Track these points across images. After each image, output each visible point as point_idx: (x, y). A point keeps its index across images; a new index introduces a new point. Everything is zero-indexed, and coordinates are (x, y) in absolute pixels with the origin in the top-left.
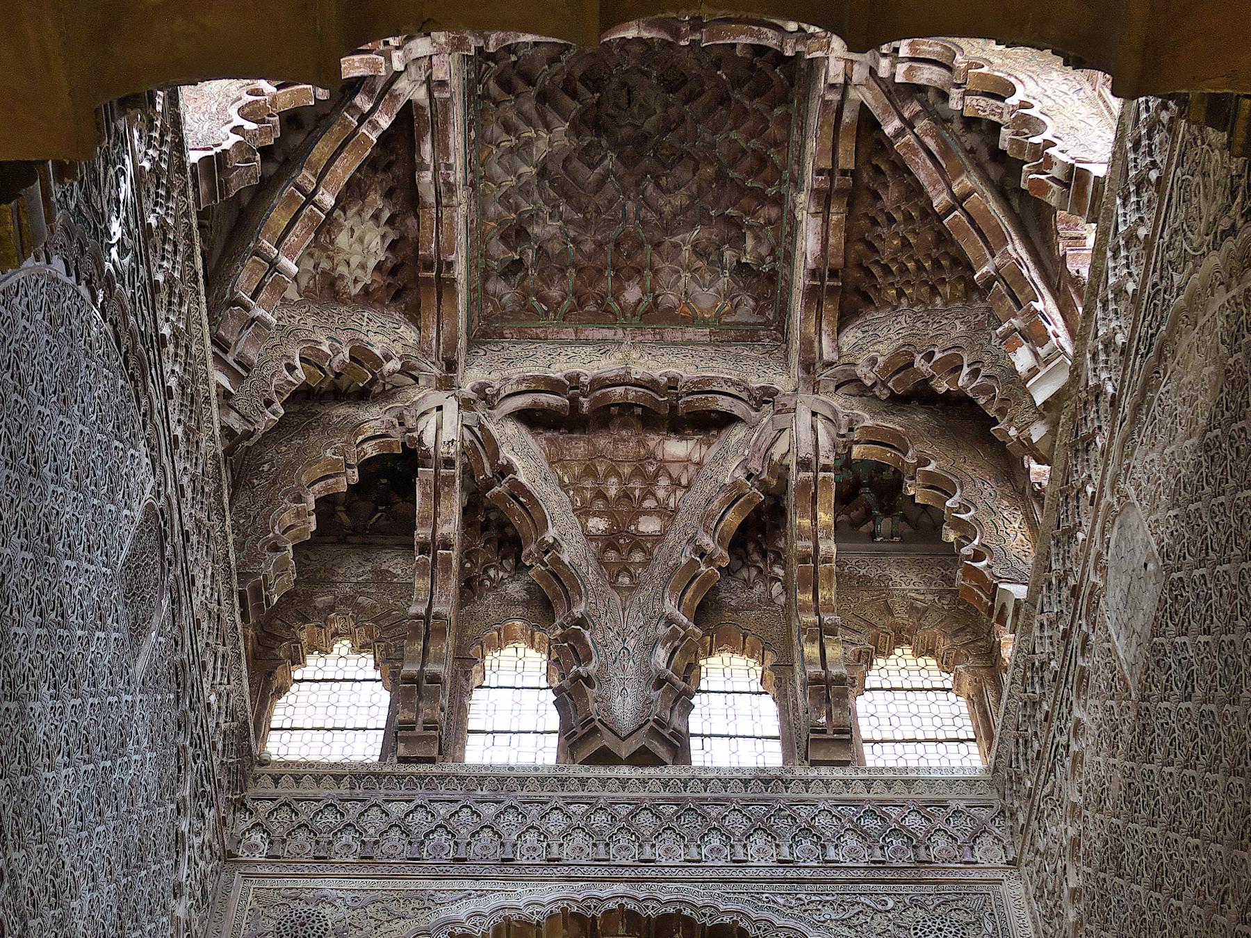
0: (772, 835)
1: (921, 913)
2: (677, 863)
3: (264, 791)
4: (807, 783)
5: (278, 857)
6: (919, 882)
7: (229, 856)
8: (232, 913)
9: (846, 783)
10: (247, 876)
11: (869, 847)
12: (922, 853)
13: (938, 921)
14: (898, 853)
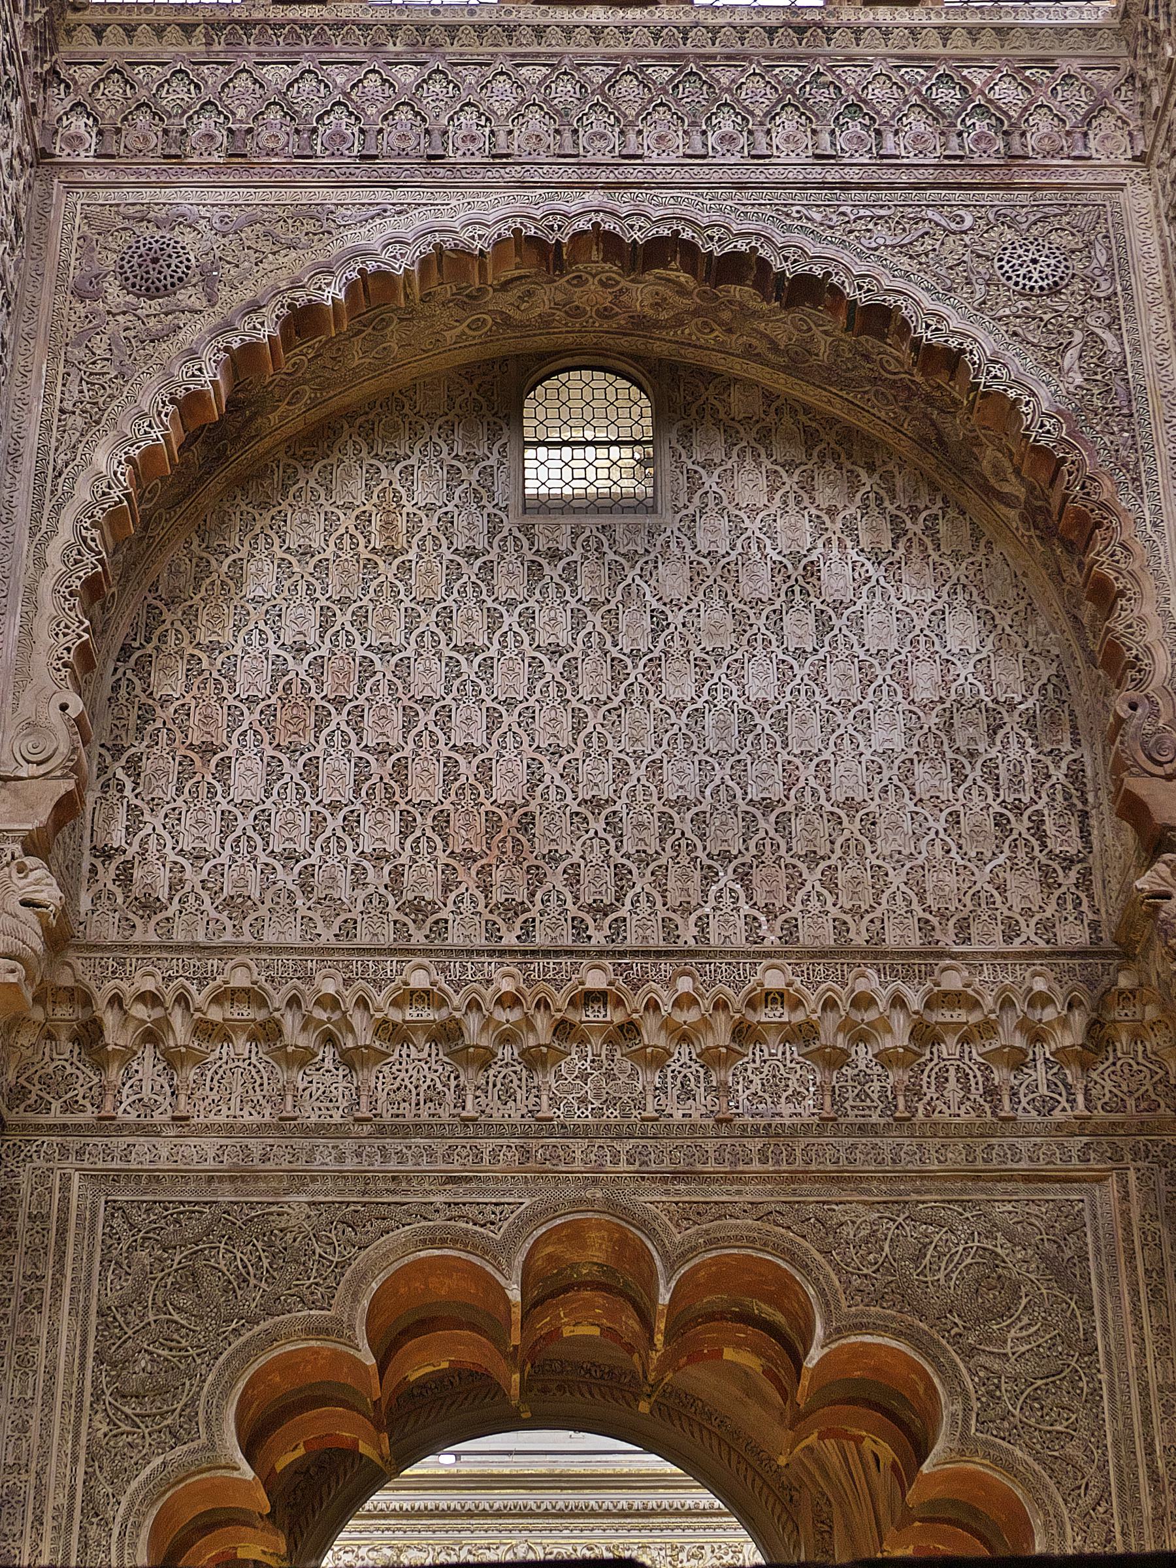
0: (802, 107)
1: (1009, 235)
3: (82, 49)
4: (858, 32)
5: (112, 157)
6: (1009, 187)
7: (43, 156)
8: (55, 244)
9: (913, 31)
10: (70, 186)
11: (942, 133)
12: (1016, 140)
13: (1032, 248)
14: (976, 138)
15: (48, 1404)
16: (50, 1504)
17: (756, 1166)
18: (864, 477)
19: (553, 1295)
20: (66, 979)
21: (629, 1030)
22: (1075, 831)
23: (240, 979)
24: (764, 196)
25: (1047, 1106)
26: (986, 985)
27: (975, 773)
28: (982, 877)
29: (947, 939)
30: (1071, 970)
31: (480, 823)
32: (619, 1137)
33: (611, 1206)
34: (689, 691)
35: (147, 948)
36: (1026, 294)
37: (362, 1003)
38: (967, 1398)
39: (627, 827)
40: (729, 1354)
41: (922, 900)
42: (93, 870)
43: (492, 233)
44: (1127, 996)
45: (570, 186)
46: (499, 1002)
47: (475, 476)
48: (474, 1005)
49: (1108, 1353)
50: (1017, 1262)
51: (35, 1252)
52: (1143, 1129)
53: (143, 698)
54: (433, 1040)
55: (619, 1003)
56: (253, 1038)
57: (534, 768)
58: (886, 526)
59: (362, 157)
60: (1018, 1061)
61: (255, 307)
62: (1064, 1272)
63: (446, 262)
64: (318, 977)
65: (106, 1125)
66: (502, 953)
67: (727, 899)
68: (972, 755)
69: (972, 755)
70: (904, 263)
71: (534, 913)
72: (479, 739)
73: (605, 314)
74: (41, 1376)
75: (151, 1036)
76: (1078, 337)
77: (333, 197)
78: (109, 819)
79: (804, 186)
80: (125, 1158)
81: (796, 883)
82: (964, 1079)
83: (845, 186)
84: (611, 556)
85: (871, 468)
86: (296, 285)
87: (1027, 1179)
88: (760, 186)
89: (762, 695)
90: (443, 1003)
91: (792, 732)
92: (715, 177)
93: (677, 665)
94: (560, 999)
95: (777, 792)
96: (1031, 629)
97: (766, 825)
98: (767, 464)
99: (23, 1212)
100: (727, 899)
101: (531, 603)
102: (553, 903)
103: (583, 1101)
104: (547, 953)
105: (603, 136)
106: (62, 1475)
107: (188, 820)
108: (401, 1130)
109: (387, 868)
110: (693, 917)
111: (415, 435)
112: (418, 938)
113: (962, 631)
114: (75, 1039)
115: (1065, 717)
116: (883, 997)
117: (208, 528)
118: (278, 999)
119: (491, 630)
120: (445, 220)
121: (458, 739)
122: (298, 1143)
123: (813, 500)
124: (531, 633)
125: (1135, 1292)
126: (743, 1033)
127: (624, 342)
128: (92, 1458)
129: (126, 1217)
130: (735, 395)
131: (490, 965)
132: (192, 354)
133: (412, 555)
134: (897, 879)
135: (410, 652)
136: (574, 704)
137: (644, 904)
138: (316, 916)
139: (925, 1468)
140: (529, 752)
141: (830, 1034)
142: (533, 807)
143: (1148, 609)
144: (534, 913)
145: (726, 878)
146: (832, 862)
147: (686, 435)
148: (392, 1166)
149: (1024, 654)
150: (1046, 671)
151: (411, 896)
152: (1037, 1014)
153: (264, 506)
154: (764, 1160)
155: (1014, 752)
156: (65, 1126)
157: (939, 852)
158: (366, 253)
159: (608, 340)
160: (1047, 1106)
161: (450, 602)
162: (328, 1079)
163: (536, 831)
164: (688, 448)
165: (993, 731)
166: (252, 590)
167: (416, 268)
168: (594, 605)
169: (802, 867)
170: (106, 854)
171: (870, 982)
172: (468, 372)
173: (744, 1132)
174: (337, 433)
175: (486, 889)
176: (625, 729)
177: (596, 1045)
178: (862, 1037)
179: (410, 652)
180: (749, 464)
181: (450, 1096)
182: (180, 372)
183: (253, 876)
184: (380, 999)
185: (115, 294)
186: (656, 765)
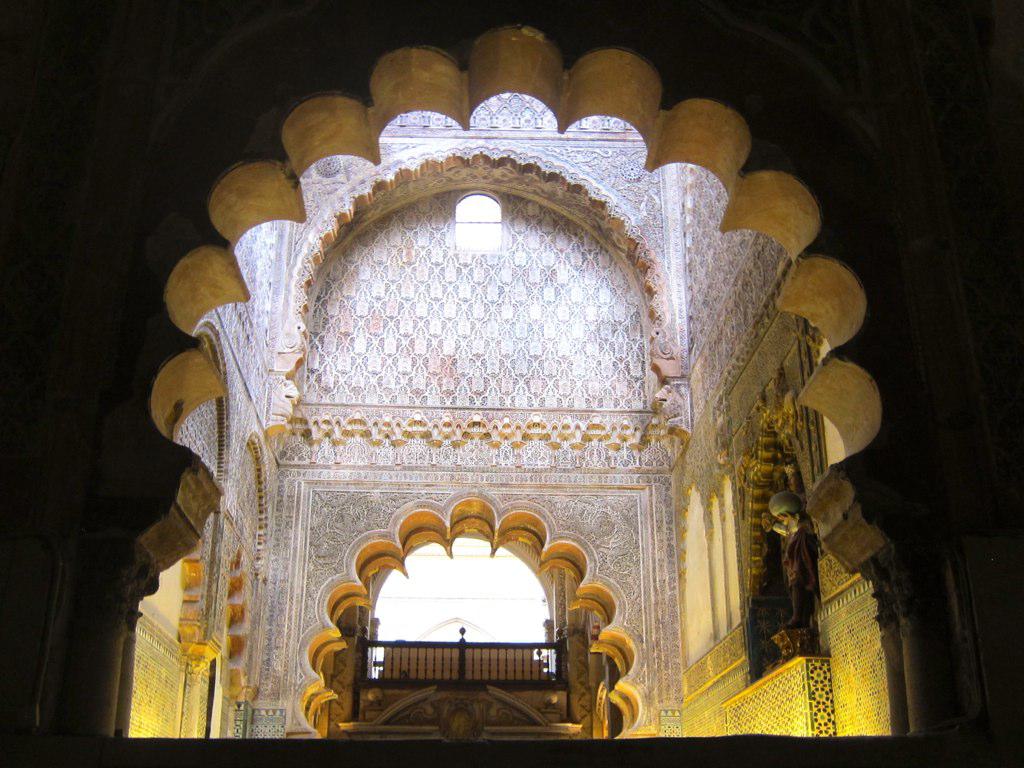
1: (624, 158)
6: (624, 141)
15: (294, 560)
20: (299, 415)
21: (487, 435)
22: (640, 369)
23: (357, 416)
25: (626, 464)
26: (608, 422)
27: (607, 347)
28: (608, 384)
29: (595, 406)
31: (439, 363)
33: (481, 495)
34: (510, 316)
35: (327, 405)
37: (398, 425)
40: (520, 539)
42: (308, 377)
44: (655, 426)
45: (472, 138)
46: (444, 425)
48: (436, 426)
49: (643, 549)
50: (614, 517)
51: (290, 509)
52: (658, 472)
53: (325, 315)
54: (422, 437)
55: (484, 426)
56: (362, 436)
57: (457, 342)
60: (618, 448)
61: (363, 182)
63: (430, 167)
65: (312, 465)
66: (445, 408)
67: (521, 391)
68: (606, 340)
69: (606, 340)
72: (439, 332)
75: (328, 435)
78: (313, 359)
79: (553, 139)
83: (568, 140)
84: (485, 266)
85: (576, 235)
87: (619, 488)
90: (425, 425)
92: (523, 135)
94: (464, 425)
97: (535, 364)
100: (521, 391)
102: (463, 391)
104: (460, 409)
105: (484, 119)
106: (299, 582)
107: (340, 360)
108: (411, 469)
109: (407, 377)
110: (509, 398)
112: (417, 403)
113: (605, 295)
114: (303, 435)
115: (639, 327)
116: (573, 426)
118: (370, 424)
120: (426, 151)
121: (432, 332)
122: (376, 472)
126: (526, 437)
127: (492, 187)
128: (309, 578)
129: (319, 496)
130: (530, 207)
133: (417, 265)
134: (579, 384)
135: (416, 300)
139: (581, 585)
141: (555, 438)
142: (457, 357)
143: (664, 299)
145: (521, 383)
147: (513, 219)
148: (408, 480)
150: (633, 311)
152: (623, 432)
153: (366, 246)
154: (532, 480)
155: (621, 339)
157: (593, 374)
159: (485, 186)
160: (626, 464)
162: (387, 450)
163: (458, 365)
167: (419, 168)
168: (479, 284)
170: (312, 371)
171: (568, 421)
172: (437, 196)
174: (391, 220)
175: (440, 385)
176: (489, 329)
177: (477, 440)
178: (565, 439)
180: (534, 233)
182: (338, 205)
184: (404, 424)
186: (499, 342)
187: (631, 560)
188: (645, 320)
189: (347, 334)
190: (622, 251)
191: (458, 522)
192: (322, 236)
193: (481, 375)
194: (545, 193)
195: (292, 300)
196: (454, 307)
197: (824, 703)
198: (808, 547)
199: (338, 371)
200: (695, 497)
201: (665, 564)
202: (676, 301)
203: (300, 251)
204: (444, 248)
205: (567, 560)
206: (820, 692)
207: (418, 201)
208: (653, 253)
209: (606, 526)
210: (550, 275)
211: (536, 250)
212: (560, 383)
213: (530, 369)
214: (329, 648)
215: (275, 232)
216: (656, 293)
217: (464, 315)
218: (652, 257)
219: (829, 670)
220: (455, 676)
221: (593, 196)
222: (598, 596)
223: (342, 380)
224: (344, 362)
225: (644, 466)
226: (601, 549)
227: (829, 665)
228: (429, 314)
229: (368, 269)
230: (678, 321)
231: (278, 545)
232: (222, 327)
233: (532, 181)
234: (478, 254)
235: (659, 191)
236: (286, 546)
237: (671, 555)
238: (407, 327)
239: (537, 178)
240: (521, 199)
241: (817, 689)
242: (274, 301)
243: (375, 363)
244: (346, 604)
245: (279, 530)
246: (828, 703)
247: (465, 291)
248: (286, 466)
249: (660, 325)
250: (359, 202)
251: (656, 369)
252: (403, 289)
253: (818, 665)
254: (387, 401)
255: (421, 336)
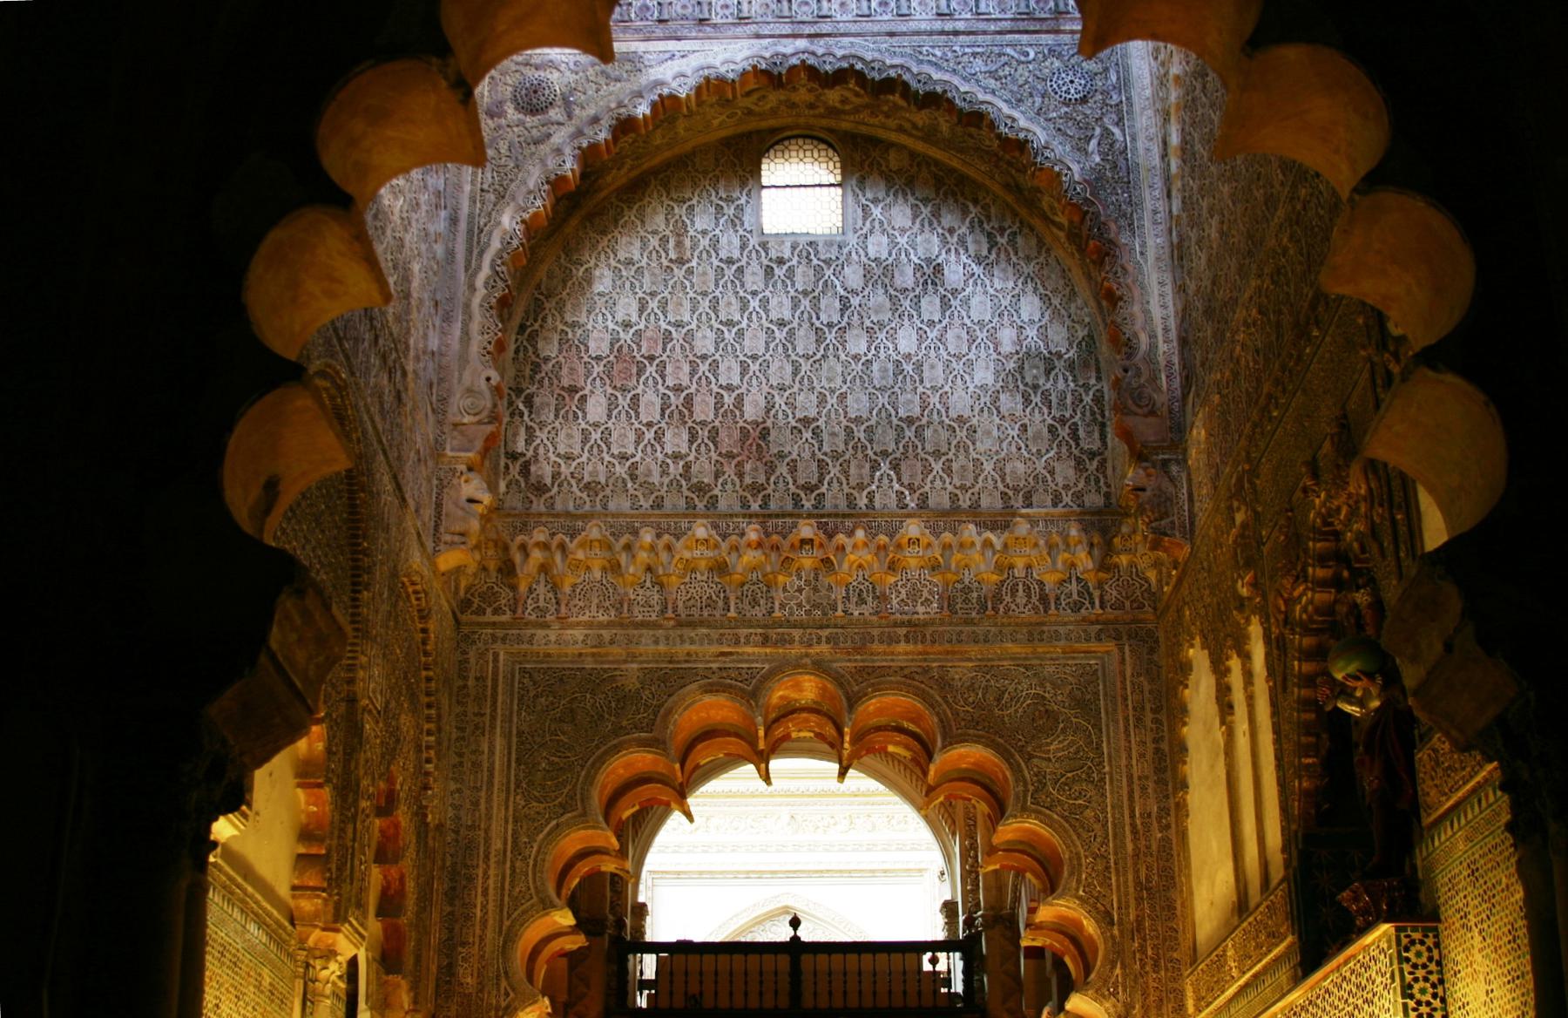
1: (1057, 64)
2: (850, 18)
6: (1057, 32)
16: (493, 848)
17: (903, 643)
18: (971, 207)
19: (784, 716)
22: (1096, 435)
23: (595, 533)
24: (905, 41)
25: (1076, 607)
27: (1036, 399)
28: (1040, 465)
29: (1018, 502)
30: (1093, 523)
31: (737, 434)
32: (821, 627)
34: (863, 348)
35: (541, 515)
36: (1067, 103)
38: (1025, 785)
39: (825, 436)
41: (1003, 480)
42: (507, 467)
43: (739, 68)
45: (787, 36)
46: (749, 545)
47: (732, 211)
53: (534, 358)
57: (769, 400)
58: (984, 240)
59: (660, 21)
61: (595, 120)
62: (1085, 705)
64: (642, 532)
66: (751, 516)
67: (886, 481)
68: (1035, 387)
70: (992, 83)
71: (769, 491)
72: (736, 381)
73: (812, 106)
74: (486, 774)
76: (1098, 131)
77: (640, 47)
78: (515, 435)
79: (931, 33)
80: (530, 642)
81: (927, 470)
82: (1027, 589)
83: (956, 33)
84: (815, 262)
85: (976, 202)
86: (620, 105)
88: (904, 34)
89: (907, 350)
91: (925, 375)
92: (876, 28)
93: (855, 332)
94: (786, 544)
95: (917, 411)
96: (1073, 306)
97: (909, 433)
98: (911, 200)
99: (472, 675)
100: (886, 481)
101: (767, 293)
102: (781, 485)
103: (800, 605)
107: (562, 435)
108: (692, 624)
111: (695, 185)
113: (1030, 307)
115: (1093, 362)
116: (978, 541)
117: (571, 251)
118: (618, 546)
119: (743, 309)
120: (710, 61)
123: (939, 223)
124: (767, 311)
125: (1126, 719)
127: (824, 122)
128: (516, 821)
130: (892, 155)
131: (743, 523)
132: (558, 151)
133: (694, 263)
134: (988, 467)
135: (693, 326)
136: (793, 357)
137: (835, 484)
138: (639, 494)
140: (766, 389)
142: (769, 424)
144: (769, 491)
145: (884, 467)
146: (951, 456)
147: (862, 183)
148: (687, 647)
149: (1068, 322)
150: (1081, 333)
151: (695, 480)
153: (604, 233)
155: (1061, 385)
156: (494, 624)
157: (1014, 449)
158: (662, 83)
159: (812, 121)
161: (717, 293)
162: (648, 593)
164: (863, 190)
165: (1048, 372)
166: (599, 287)
168: (805, 293)
169: (931, 459)
170: (514, 456)
172: (727, 143)
173: (896, 625)
174: (647, 184)
175: (741, 475)
176: (824, 373)
179: (693, 326)
180: (900, 200)
181: (721, 603)
182: (551, 163)
183: (601, 468)
184: (679, 545)
185: (510, 109)
186: (843, 397)
187: (1089, 780)
188: (1104, 349)
189: (573, 390)
190: (1060, 227)
191: (776, 720)
192: (526, 216)
193: (813, 454)
194: (921, 130)
195: (475, 327)
196: (763, 336)
197: (1428, 1004)
198: (1396, 733)
199: (559, 455)
200: (1197, 655)
201: (1151, 785)
202: (1157, 312)
203: (488, 245)
204: (741, 232)
205: (976, 782)
206: (1421, 984)
207: (693, 153)
208: (1113, 226)
209: (1044, 720)
210: (932, 274)
211: (903, 232)
212: (955, 466)
213: (906, 440)
214: (556, 946)
215: (443, 213)
216: (1121, 298)
217: (780, 349)
218: (1112, 235)
219: (1437, 945)
220: (784, 1002)
221: (1003, 130)
222: (1031, 846)
223: (565, 470)
224: (567, 439)
225: (1109, 610)
226: (1035, 761)
227: (1436, 936)
228: (717, 350)
229: (606, 272)
230: (1162, 347)
231: (461, 764)
232: (353, 374)
233: (896, 107)
234: (803, 241)
235: (1121, 119)
236: (476, 765)
237: (1159, 770)
238: (678, 373)
239: (902, 103)
240: (874, 142)
241: (1416, 980)
242: (443, 333)
243: (624, 439)
244: (584, 868)
245: (463, 738)
246: (1437, 1003)
247: (781, 307)
248: (472, 624)
249: (1129, 356)
250: (589, 157)
251: (1126, 435)
252: (670, 307)
253: (1417, 936)
254: (646, 504)
255: (704, 390)
